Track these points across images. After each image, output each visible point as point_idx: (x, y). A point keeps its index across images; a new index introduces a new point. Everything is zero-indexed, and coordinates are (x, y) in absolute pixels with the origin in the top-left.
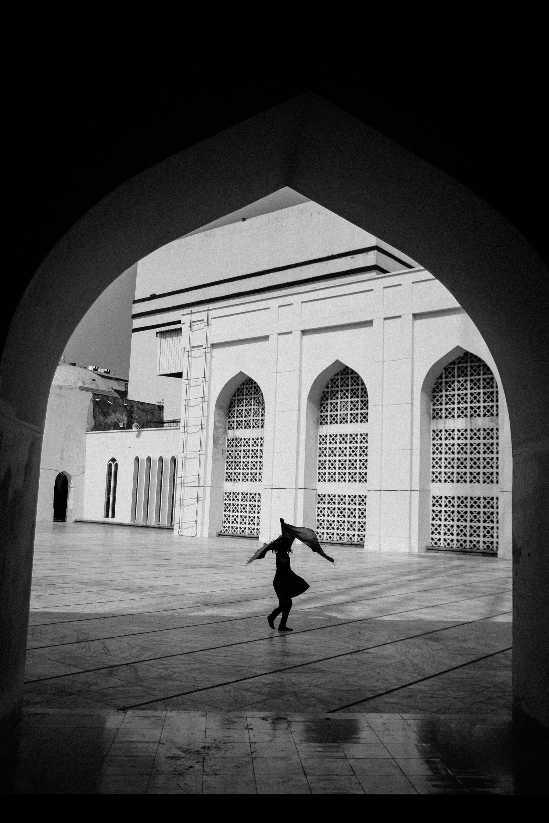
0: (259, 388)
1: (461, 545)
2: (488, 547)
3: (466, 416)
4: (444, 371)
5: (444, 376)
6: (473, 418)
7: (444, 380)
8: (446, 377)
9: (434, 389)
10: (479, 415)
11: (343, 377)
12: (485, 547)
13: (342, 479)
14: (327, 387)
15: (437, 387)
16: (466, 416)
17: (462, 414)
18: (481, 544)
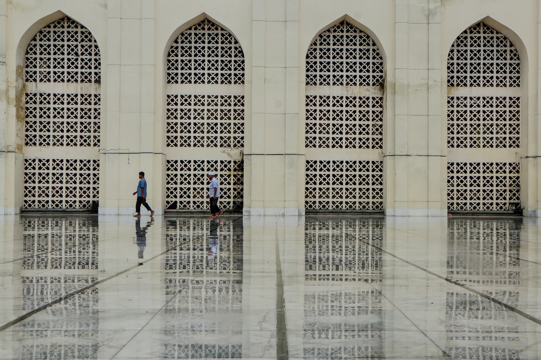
0: (90, 33)
1: (337, 206)
2: (351, 207)
3: (342, 84)
4: (319, 38)
5: (318, 43)
6: (349, 86)
7: (318, 47)
8: (321, 44)
9: (307, 55)
10: (355, 84)
11: (197, 32)
12: (361, 207)
13: (198, 143)
14: (176, 42)
15: (311, 53)
16: (342, 84)
17: (338, 81)
18: (344, 204)
